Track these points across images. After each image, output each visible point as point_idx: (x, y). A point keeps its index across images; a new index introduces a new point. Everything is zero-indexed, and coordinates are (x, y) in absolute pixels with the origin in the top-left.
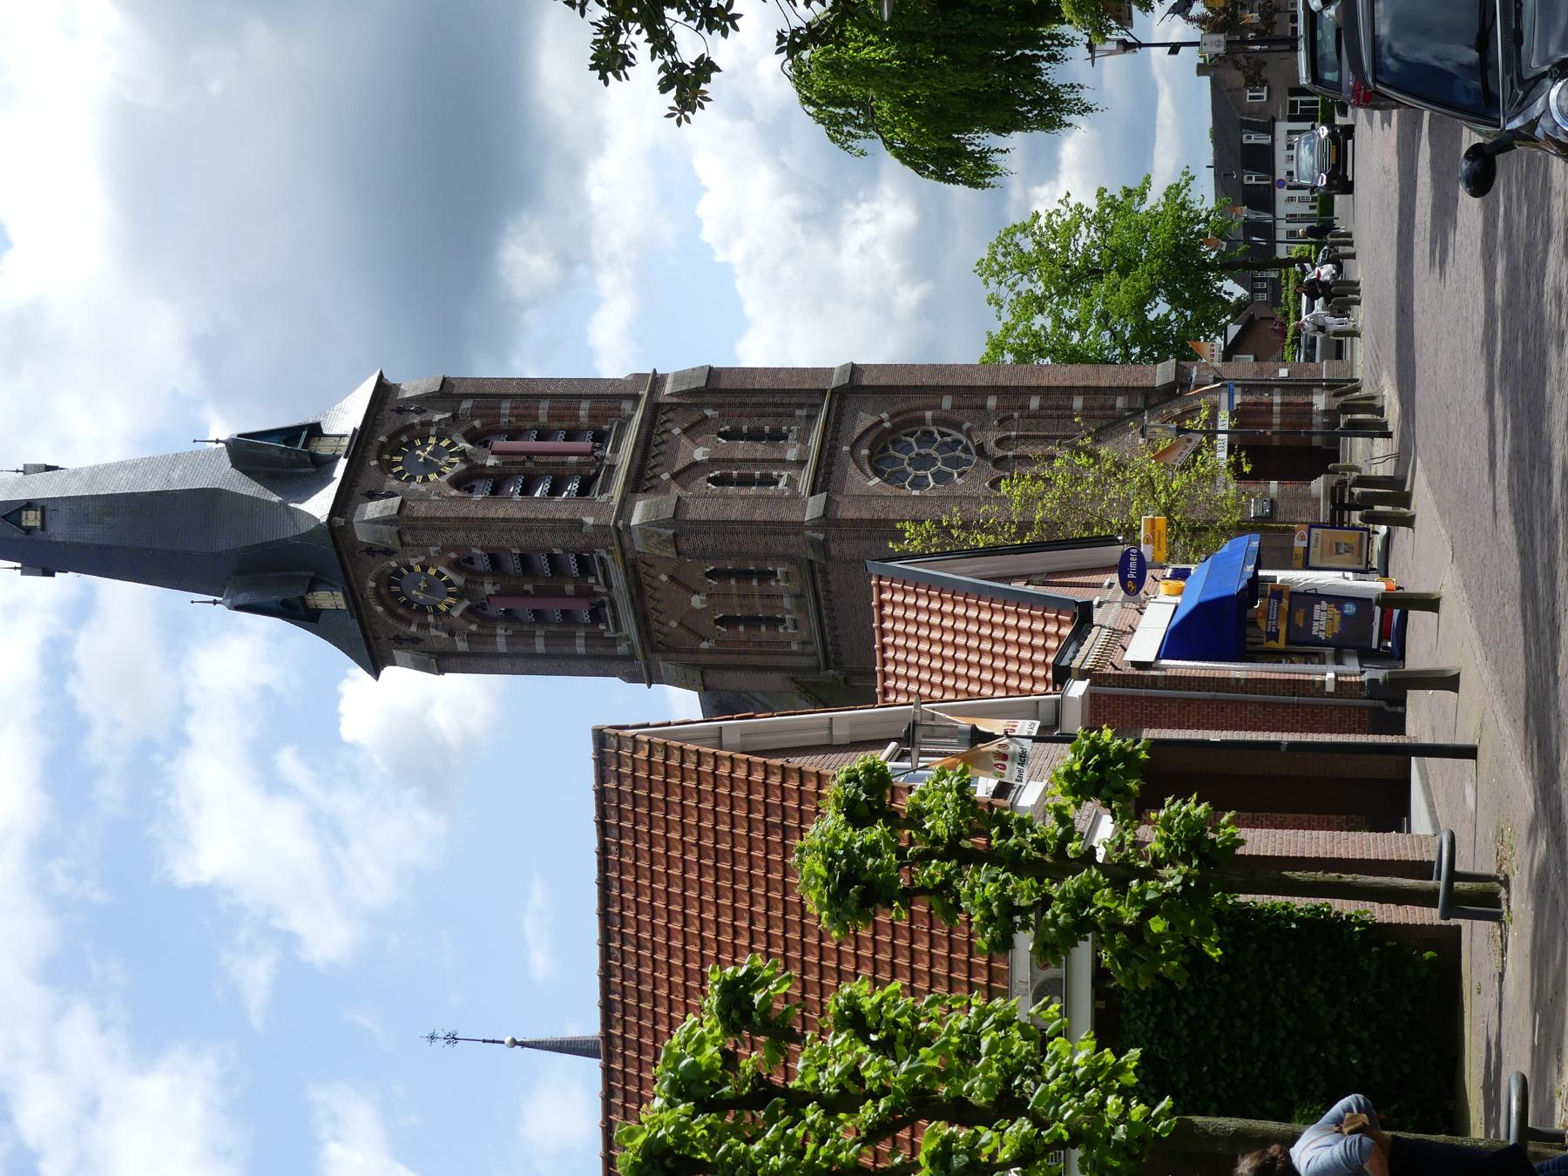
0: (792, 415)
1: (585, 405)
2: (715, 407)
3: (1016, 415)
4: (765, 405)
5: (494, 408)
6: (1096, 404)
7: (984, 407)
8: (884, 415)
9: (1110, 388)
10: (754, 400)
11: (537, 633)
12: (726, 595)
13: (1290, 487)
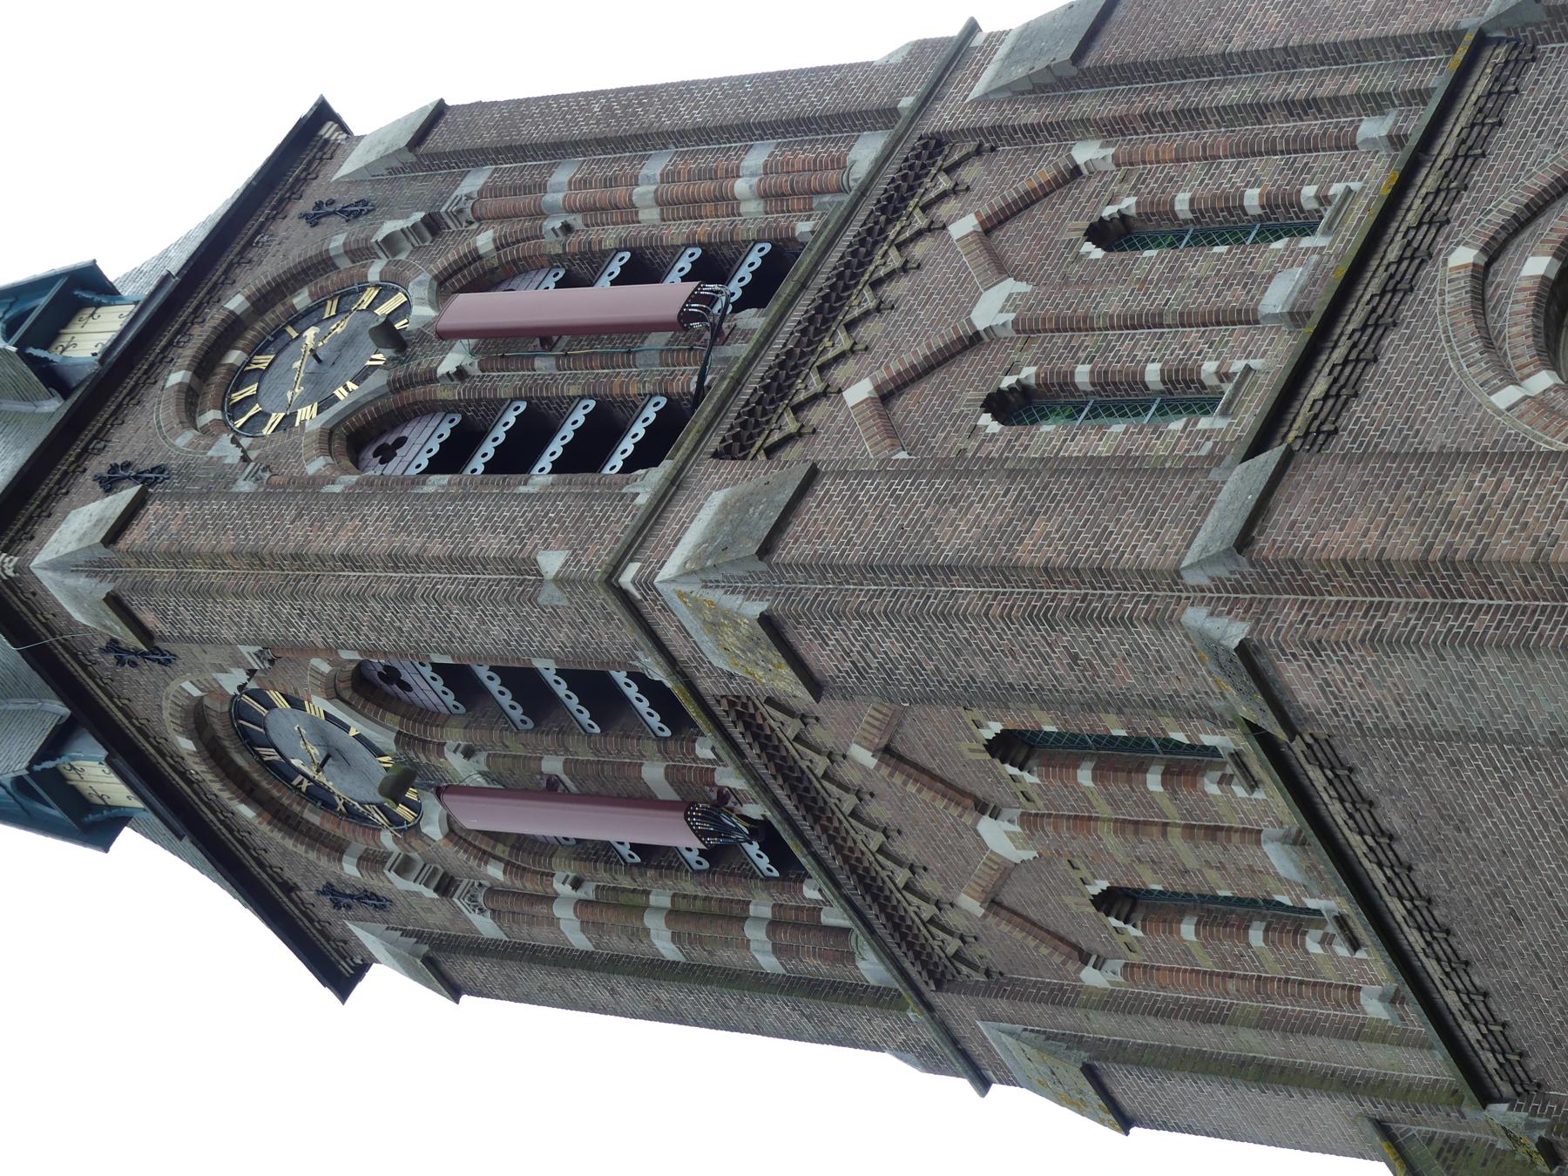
0: (1346, 143)
1: (756, 157)
2: (1110, 129)
4: (1260, 110)
5: (527, 190)
10: (1229, 95)
11: (653, 900)
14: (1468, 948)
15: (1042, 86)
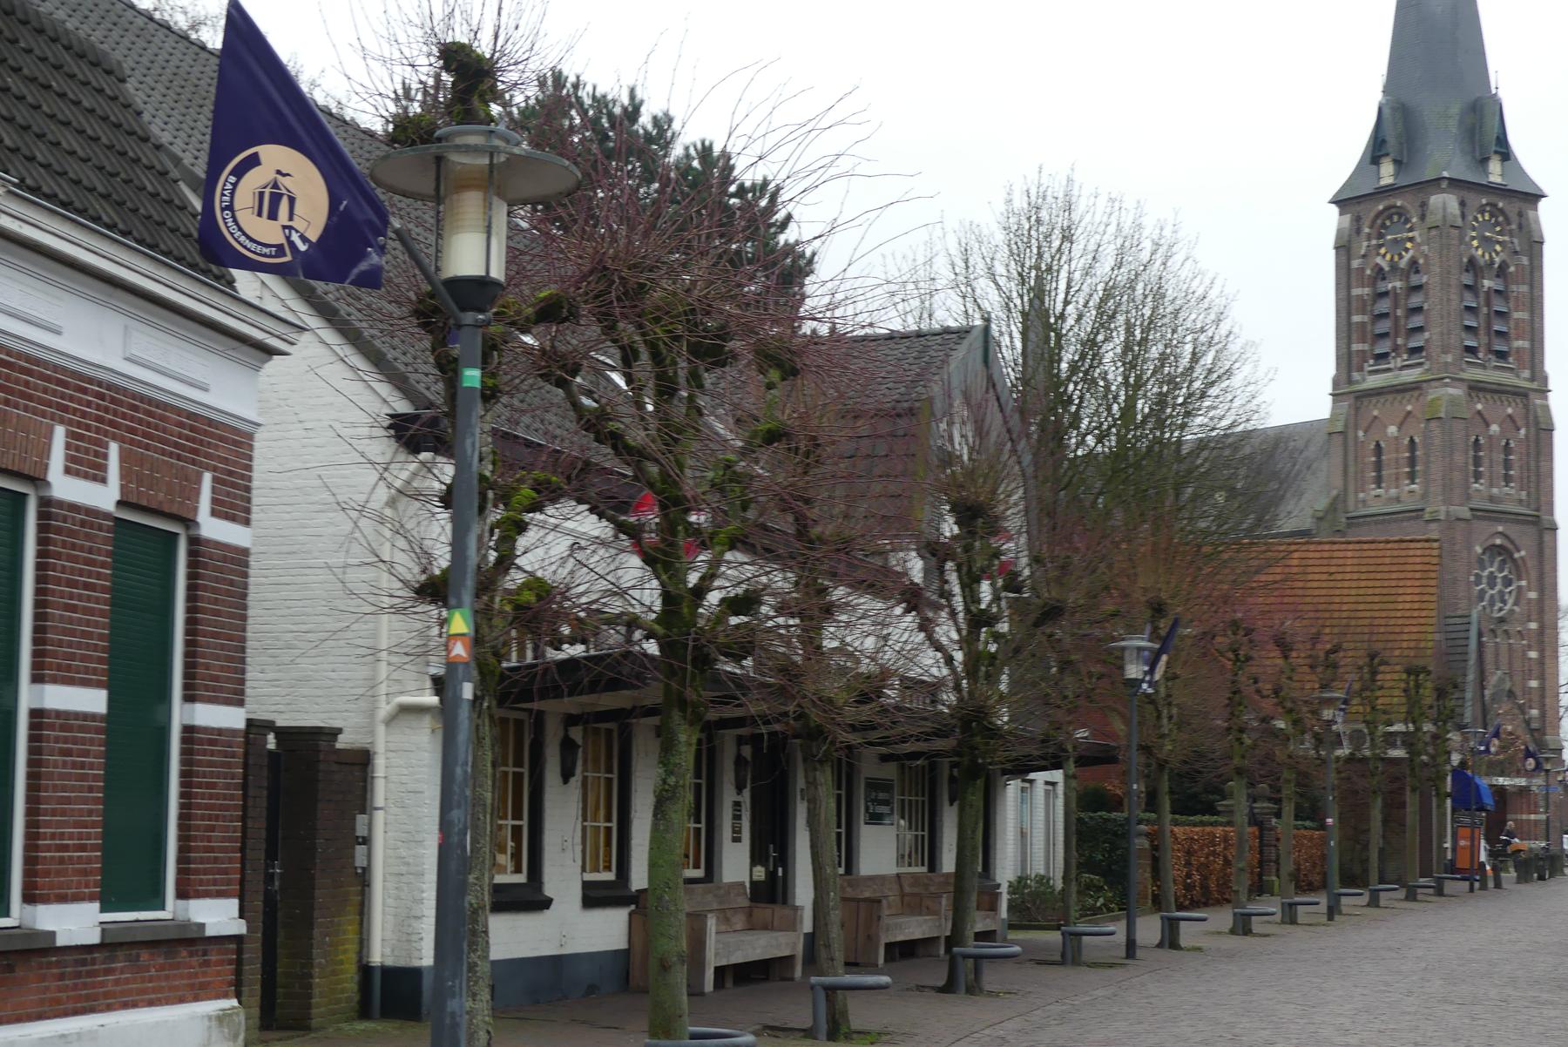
2: (1527, 436)
4: (1528, 470)
8: (1523, 553)
9: (1544, 705)
12: (1397, 451)
15: (1537, 423)
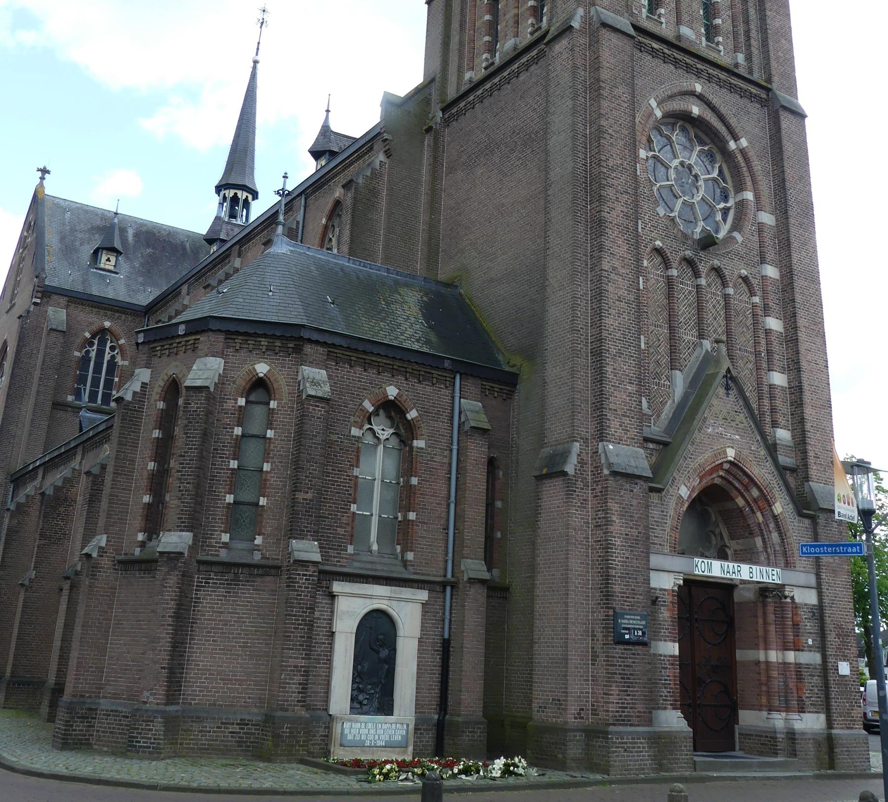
3: (756, 299)
6: (778, 402)
7: (763, 261)
9: (802, 421)
13: (670, 675)
14: (486, 102)
